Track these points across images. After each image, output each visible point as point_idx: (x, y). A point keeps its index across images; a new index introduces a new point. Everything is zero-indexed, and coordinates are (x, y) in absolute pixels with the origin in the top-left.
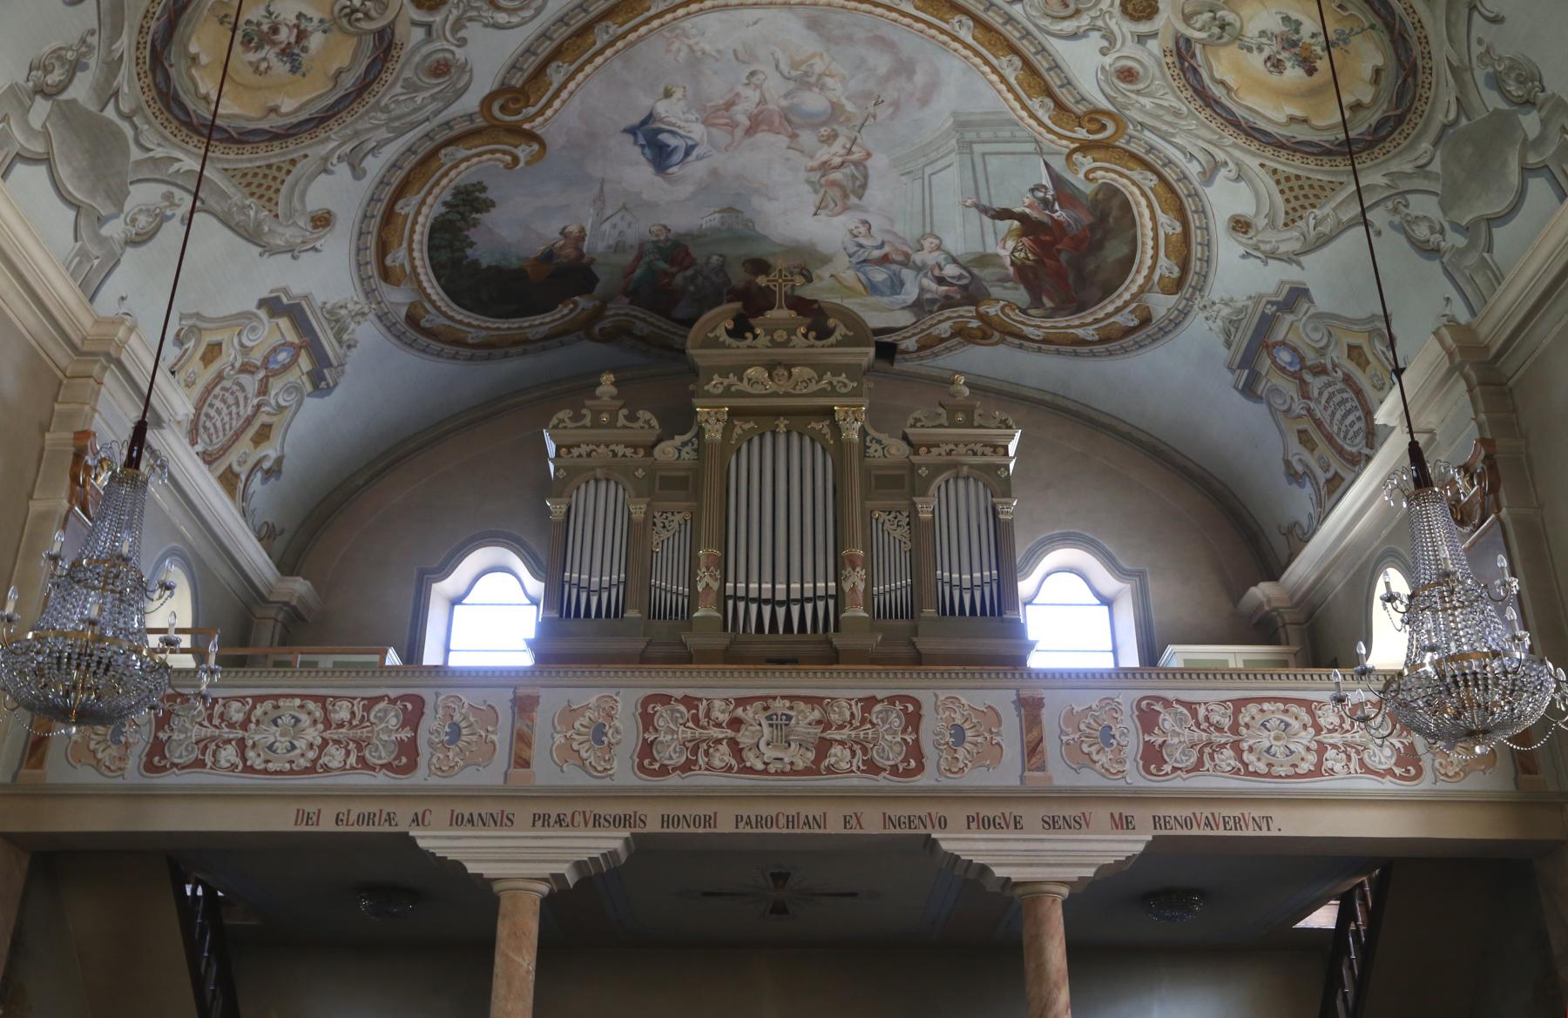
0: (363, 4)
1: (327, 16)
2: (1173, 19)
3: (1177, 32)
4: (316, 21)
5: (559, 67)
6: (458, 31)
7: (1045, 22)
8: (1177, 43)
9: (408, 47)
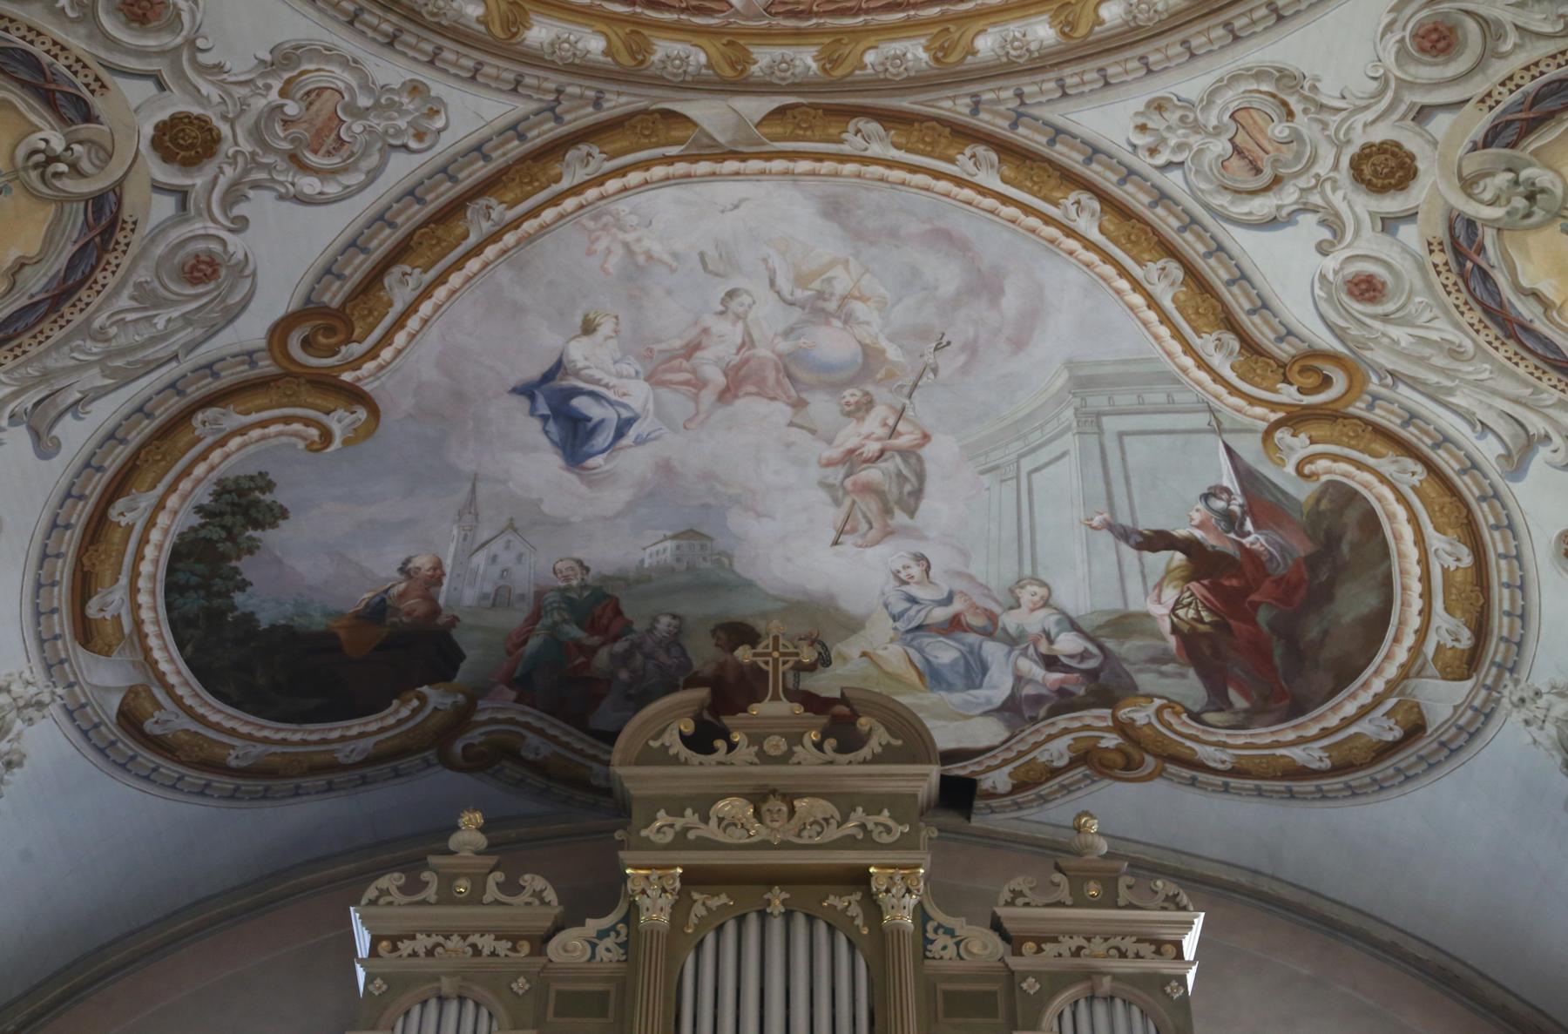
0: (68, 148)
2: (1442, 187)
3: (1451, 209)
5: (405, 274)
6: (236, 203)
7: (1222, 201)
8: (1451, 229)
9: (145, 229)
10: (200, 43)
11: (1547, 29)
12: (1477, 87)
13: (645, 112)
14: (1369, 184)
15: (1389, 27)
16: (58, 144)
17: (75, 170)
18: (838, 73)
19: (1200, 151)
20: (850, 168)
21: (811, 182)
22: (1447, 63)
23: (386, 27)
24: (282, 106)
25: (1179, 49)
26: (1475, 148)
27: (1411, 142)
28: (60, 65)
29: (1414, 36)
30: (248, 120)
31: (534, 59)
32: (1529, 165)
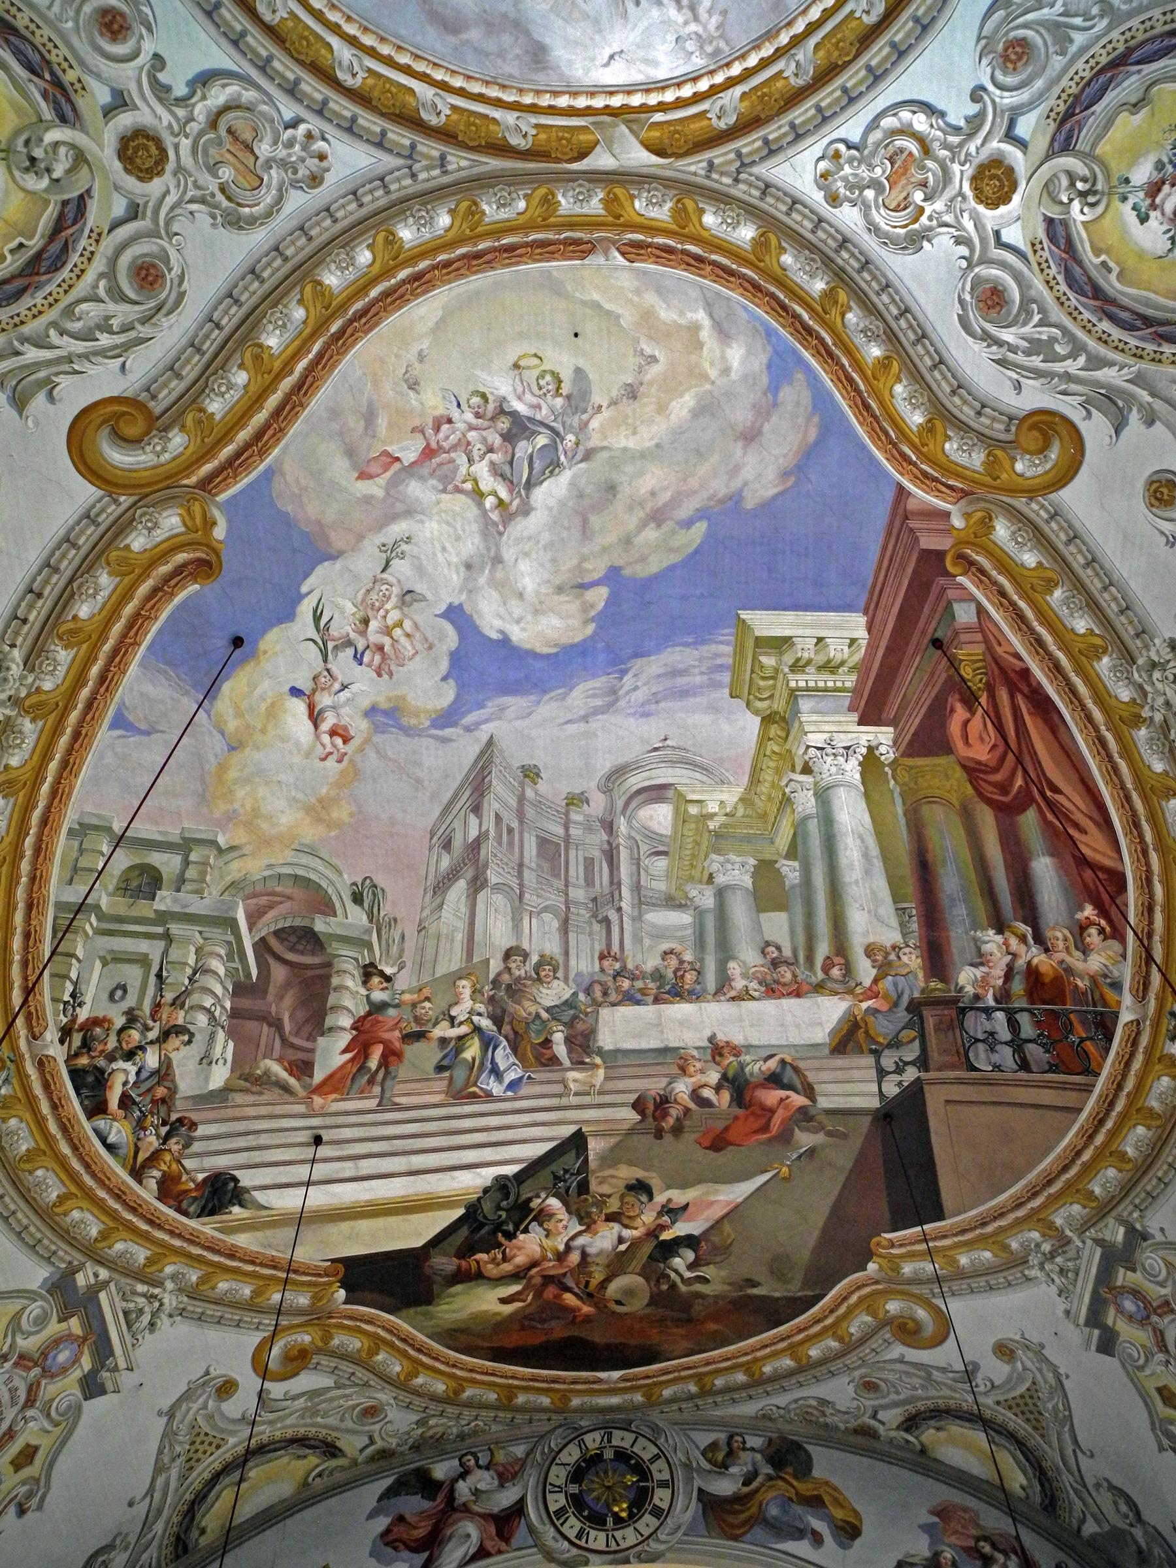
0: (1071, 200)
1: (1116, 202)
2: (96, 148)
3: (83, 129)
4: (1131, 201)
5: (868, 12)
6: (975, 116)
7: (249, 95)
8: (75, 110)
9: (1042, 109)
10: (964, 264)
11: (84, 306)
12: (108, 244)
13: (678, 156)
14: (148, 137)
15: (182, 278)
16: (1076, 205)
17: (1072, 178)
18: (542, 191)
19: (275, 143)
20: (528, 100)
21: (556, 84)
22: (135, 259)
23: (845, 255)
24: (925, 200)
25: (313, 233)
26: (88, 191)
27: (131, 182)
28: (1054, 270)
29: (163, 276)
30: (949, 193)
31: (752, 212)
32: (46, 190)
